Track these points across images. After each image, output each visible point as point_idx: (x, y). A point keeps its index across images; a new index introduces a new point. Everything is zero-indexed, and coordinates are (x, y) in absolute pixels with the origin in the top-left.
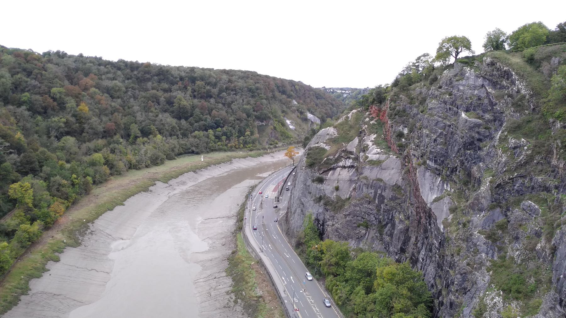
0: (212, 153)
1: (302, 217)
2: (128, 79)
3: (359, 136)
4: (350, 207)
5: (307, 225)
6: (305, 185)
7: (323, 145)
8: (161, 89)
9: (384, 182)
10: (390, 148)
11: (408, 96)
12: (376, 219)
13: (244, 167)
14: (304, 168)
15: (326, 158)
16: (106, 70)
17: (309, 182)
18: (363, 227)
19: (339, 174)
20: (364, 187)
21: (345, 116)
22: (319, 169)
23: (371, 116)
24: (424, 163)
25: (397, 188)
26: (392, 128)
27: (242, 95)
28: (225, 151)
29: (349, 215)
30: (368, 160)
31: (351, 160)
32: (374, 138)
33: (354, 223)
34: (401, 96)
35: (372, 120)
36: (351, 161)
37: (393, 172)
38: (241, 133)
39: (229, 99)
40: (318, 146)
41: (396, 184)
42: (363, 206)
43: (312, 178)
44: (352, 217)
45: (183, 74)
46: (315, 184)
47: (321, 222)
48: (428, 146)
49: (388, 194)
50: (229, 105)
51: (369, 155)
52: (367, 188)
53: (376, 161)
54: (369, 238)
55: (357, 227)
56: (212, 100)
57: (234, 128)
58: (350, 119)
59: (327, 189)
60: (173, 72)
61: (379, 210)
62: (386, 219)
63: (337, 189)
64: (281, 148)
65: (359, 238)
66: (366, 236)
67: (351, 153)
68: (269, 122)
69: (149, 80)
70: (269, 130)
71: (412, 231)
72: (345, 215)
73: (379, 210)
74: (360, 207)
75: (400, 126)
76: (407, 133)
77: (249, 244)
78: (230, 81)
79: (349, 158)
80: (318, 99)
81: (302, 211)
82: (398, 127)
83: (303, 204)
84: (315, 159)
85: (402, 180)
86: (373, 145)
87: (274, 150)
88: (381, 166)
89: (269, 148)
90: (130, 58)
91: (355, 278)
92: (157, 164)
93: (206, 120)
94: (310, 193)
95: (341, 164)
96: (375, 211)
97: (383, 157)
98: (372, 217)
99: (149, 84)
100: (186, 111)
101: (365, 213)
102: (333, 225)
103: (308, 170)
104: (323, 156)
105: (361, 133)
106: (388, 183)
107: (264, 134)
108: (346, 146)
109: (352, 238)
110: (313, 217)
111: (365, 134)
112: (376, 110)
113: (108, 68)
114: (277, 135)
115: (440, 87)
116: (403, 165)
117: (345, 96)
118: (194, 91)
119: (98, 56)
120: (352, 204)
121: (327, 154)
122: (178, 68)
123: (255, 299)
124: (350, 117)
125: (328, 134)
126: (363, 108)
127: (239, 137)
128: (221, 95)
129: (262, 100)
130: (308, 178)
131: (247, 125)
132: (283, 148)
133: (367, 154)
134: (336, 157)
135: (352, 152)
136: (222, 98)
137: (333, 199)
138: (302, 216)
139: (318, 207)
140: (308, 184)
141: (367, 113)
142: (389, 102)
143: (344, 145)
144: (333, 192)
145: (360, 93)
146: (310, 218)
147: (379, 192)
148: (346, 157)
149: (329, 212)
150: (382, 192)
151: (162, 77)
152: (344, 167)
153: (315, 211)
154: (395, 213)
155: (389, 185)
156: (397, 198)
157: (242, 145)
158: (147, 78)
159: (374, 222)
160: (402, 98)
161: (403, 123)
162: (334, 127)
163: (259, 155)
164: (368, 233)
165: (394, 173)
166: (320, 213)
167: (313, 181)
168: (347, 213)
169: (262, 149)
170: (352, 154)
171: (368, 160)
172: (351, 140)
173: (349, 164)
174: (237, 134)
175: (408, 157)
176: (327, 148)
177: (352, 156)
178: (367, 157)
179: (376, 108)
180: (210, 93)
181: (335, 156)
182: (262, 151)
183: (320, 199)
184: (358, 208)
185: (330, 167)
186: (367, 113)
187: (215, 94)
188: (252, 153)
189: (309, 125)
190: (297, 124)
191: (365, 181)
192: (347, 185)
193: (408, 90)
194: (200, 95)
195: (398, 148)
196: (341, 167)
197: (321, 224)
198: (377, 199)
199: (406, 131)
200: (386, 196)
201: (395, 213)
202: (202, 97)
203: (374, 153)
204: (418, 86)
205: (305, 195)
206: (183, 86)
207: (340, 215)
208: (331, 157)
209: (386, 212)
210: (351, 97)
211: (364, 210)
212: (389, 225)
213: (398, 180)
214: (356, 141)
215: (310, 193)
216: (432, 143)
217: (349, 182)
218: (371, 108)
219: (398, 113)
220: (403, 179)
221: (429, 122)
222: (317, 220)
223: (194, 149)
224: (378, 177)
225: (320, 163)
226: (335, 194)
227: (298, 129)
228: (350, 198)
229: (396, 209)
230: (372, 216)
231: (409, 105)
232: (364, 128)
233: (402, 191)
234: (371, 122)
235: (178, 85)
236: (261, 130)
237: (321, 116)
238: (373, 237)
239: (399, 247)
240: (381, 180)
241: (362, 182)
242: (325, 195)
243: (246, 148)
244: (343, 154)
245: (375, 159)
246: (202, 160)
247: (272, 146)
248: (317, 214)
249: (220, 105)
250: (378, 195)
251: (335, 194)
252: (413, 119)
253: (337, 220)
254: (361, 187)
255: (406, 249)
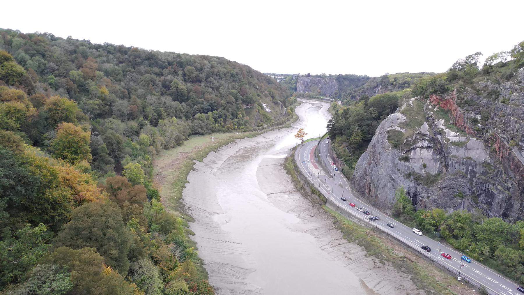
0: (214, 134)
1: (393, 191)
2: (121, 62)
3: (427, 121)
4: (444, 181)
5: (399, 197)
6: (393, 163)
7: (398, 129)
8: (153, 73)
9: (473, 160)
10: (464, 131)
11: (475, 89)
12: (469, 190)
13: (248, 147)
14: (390, 148)
15: (405, 140)
16: (98, 53)
17: (397, 161)
18: (459, 198)
19: (421, 154)
20: (456, 164)
21: (406, 103)
22: (402, 150)
23: (432, 104)
24: (517, 144)
25: (486, 164)
26: (464, 115)
27: (226, 80)
28: (223, 132)
29: (445, 188)
30: (450, 141)
31: (426, 141)
32: (444, 123)
33: (451, 195)
34: (466, 88)
35: (435, 108)
36: (426, 142)
37: (478, 151)
38: (235, 116)
39: (216, 84)
40: (394, 130)
41: (485, 161)
42: (458, 180)
43: (398, 157)
44: (448, 190)
45: (169, 59)
46: (403, 163)
47: (412, 195)
48: (519, 130)
49: (479, 170)
50: (218, 89)
51: (449, 138)
52: (459, 165)
53: (458, 142)
54: (465, 206)
55: (453, 197)
56: (203, 84)
57: (227, 111)
58: (412, 106)
59: (416, 166)
60: (160, 57)
61: (472, 184)
62: (480, 191)
63: (425, 166)
64: (267, 130)
65: (456, 207)
66: (462, 205)
67: (425, 135)
68: (253, 105)
69: (141, 63)
70: (254, 112)
71: (515, 199)
72: (441, 188)
73: (472, 184)
74: (455, 181)
75: (471, 113)
76: (481, 119)
77: (350, 215)
78: (212, 67)
79: (424, 139)
80: (269, 84)
81: (393, 185)
82: (470, 114)
83: (393, 180)
84: (397, 141)
85: (490, 158)
86: (446, 129)
87: (263, 131)
88: (466, 146)
89: (258, 129)
90: (116, 42)
91: (489, 239)
92: (180, 144)
93: (202, 103)
94: (399, 170)
95: (419, 144)
96: (469, 184)
97: (463, 139)
98: (466, 189)
99: (142, 68)
100: (184, 95)
101: (460, 185)
102: (428, 197)
103: (394, 150)
104: (403, 138)
105: (428, 118)
106: (477, 160)
107: (251, 116)
108: (419, 130)
109: (449, 207)
110: (405, 191)
111: (433, 120)
112: (438, 99)
113: (100, 51)
114: (261, 118)
115: (520, 82)
116: (487, 147)
117: (278, 81)
118: (184, 75)
119: (86, 39)
120: (447, 179)
121: (406, 136)
122: (166, 54)
123: (401, 259)
124: (412, 104)
125: (398, 119)
126: (421, 97)
127: (232, 119)
128: (208, 80)
129: (245, 85)
130: (396, 158)
131: (238, 108)
132: (269, 130)
133: (447, 137)
134: (414, 139)
135: (426, 135)
136: (210, 82)
137: (423, 175)
138: (394, 190)
139: (409, 182)
140: (396, 162)
141: (428, 101)
142: (455, 93)
143: (417, 128)
144: (421, 169)
145: (292, 79)
146: (402, 191)
147: (471, 168)
148: (421, 139)
149: (421, 186)
150: (473, 168)
151: (152, 61)
152: (423, 148)
153: (406, 185)
154: (489, 185)
155: (479, 162)
156: (488, 173)
157: (236, 127)
158: (138, 63)
159: (468, 193)
160: (468, 90)
161: (474, 110)
162: (401, 113)
163: (254, 136)
164: (463, 203)
165: (480, 153)
166: (411, 187)
167: (400, 160)
168: (442, 186)
169: (254, 130)
170: (427, 137)
171: (450, 141)
172: (421, 124)
173: (427, 145)
174: (231, 117)
175: (491, 139)
176: (402, 131)
177: (426, 138)
178: (449, 140)
179: (438, 97)
180: (199, 78)
181: (413, 138)
182: (254, 132)
183: (410, 175)
184: (454, 182)
185: (410, 147)
186: (428, 101)
187: (204, 79)
188: (247, 134)
189: (280, 108)
190: (271, 107)
191: (456, 159)
192: (432, 162)
193: (471, 83)
194: (190, 80)
195: (475, 131)
196: (420, 148)
197: (412, 196)
198: (469, 174)
199: (479, 117)
200: (477, 171)
201: (489, 185)
202: (192, 82)
203: (452, 136)
204: (481, 80)
205: (394, 172)
206: (174, 70)
207: (434, 188)
208: (410, 139)
209: (478, 184)
210: (285, 82)
211: (459, 183)
212: (484, 195)
213: (485, 159)
214: (426, 125)
215: (399, 170)
216: (522, 128)
217: (433, 160)
218: (431, 97)
219: (467, 102)
220: (491, 157)
221: (514, 110)
222: (409, 193)
223: (199, 130)
224: (467, 155)
225: (402, 144)
226: (423, 171)
227: (273, 112)
228: (439, 174)
229: (488, 182)
230: (466, 188)
231: (476, 96)
232: (430, 114)
233: (492, 167)
234: (435, 109)
235: (168, 70)
236: (248, 112)
237: (282, 100)
238: (469, 205)
239: (501, 213)
240: (470, 158)
241: (453, 160)
242: (414, 172)
243: (240, 129)
244: (418, 136)
245: (457, 141)
246: (213, 141)
247: (260, 128)
248: (409, 188)
249: (210, 90)
250: (470, 171)
251: (423, 171)
252: (483, 107)
253: (432, 192)
254: (454, 164)
255: (509, 213)
